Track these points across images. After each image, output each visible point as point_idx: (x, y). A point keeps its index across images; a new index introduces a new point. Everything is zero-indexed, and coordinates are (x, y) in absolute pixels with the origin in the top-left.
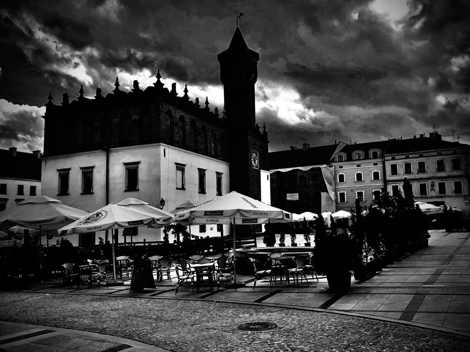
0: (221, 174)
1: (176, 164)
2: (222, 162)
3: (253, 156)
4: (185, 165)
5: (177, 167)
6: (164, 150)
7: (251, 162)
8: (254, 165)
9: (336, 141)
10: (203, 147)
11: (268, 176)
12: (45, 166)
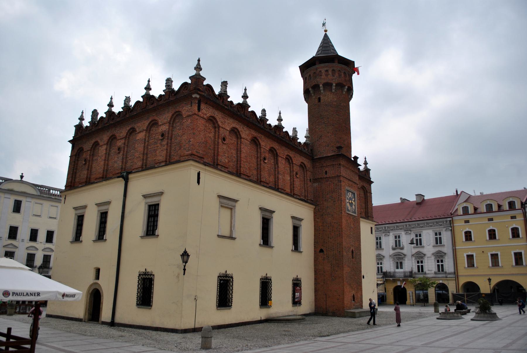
0: (301, 220)
3: (348, 196)
4: (236, 201)
5: (220, 202)
6: (199, 174)
7: (345, 205)
8: (349, 208)
9: (457, 191)
10: (272, 179)
11: (371, 228)
12: (64, 203)
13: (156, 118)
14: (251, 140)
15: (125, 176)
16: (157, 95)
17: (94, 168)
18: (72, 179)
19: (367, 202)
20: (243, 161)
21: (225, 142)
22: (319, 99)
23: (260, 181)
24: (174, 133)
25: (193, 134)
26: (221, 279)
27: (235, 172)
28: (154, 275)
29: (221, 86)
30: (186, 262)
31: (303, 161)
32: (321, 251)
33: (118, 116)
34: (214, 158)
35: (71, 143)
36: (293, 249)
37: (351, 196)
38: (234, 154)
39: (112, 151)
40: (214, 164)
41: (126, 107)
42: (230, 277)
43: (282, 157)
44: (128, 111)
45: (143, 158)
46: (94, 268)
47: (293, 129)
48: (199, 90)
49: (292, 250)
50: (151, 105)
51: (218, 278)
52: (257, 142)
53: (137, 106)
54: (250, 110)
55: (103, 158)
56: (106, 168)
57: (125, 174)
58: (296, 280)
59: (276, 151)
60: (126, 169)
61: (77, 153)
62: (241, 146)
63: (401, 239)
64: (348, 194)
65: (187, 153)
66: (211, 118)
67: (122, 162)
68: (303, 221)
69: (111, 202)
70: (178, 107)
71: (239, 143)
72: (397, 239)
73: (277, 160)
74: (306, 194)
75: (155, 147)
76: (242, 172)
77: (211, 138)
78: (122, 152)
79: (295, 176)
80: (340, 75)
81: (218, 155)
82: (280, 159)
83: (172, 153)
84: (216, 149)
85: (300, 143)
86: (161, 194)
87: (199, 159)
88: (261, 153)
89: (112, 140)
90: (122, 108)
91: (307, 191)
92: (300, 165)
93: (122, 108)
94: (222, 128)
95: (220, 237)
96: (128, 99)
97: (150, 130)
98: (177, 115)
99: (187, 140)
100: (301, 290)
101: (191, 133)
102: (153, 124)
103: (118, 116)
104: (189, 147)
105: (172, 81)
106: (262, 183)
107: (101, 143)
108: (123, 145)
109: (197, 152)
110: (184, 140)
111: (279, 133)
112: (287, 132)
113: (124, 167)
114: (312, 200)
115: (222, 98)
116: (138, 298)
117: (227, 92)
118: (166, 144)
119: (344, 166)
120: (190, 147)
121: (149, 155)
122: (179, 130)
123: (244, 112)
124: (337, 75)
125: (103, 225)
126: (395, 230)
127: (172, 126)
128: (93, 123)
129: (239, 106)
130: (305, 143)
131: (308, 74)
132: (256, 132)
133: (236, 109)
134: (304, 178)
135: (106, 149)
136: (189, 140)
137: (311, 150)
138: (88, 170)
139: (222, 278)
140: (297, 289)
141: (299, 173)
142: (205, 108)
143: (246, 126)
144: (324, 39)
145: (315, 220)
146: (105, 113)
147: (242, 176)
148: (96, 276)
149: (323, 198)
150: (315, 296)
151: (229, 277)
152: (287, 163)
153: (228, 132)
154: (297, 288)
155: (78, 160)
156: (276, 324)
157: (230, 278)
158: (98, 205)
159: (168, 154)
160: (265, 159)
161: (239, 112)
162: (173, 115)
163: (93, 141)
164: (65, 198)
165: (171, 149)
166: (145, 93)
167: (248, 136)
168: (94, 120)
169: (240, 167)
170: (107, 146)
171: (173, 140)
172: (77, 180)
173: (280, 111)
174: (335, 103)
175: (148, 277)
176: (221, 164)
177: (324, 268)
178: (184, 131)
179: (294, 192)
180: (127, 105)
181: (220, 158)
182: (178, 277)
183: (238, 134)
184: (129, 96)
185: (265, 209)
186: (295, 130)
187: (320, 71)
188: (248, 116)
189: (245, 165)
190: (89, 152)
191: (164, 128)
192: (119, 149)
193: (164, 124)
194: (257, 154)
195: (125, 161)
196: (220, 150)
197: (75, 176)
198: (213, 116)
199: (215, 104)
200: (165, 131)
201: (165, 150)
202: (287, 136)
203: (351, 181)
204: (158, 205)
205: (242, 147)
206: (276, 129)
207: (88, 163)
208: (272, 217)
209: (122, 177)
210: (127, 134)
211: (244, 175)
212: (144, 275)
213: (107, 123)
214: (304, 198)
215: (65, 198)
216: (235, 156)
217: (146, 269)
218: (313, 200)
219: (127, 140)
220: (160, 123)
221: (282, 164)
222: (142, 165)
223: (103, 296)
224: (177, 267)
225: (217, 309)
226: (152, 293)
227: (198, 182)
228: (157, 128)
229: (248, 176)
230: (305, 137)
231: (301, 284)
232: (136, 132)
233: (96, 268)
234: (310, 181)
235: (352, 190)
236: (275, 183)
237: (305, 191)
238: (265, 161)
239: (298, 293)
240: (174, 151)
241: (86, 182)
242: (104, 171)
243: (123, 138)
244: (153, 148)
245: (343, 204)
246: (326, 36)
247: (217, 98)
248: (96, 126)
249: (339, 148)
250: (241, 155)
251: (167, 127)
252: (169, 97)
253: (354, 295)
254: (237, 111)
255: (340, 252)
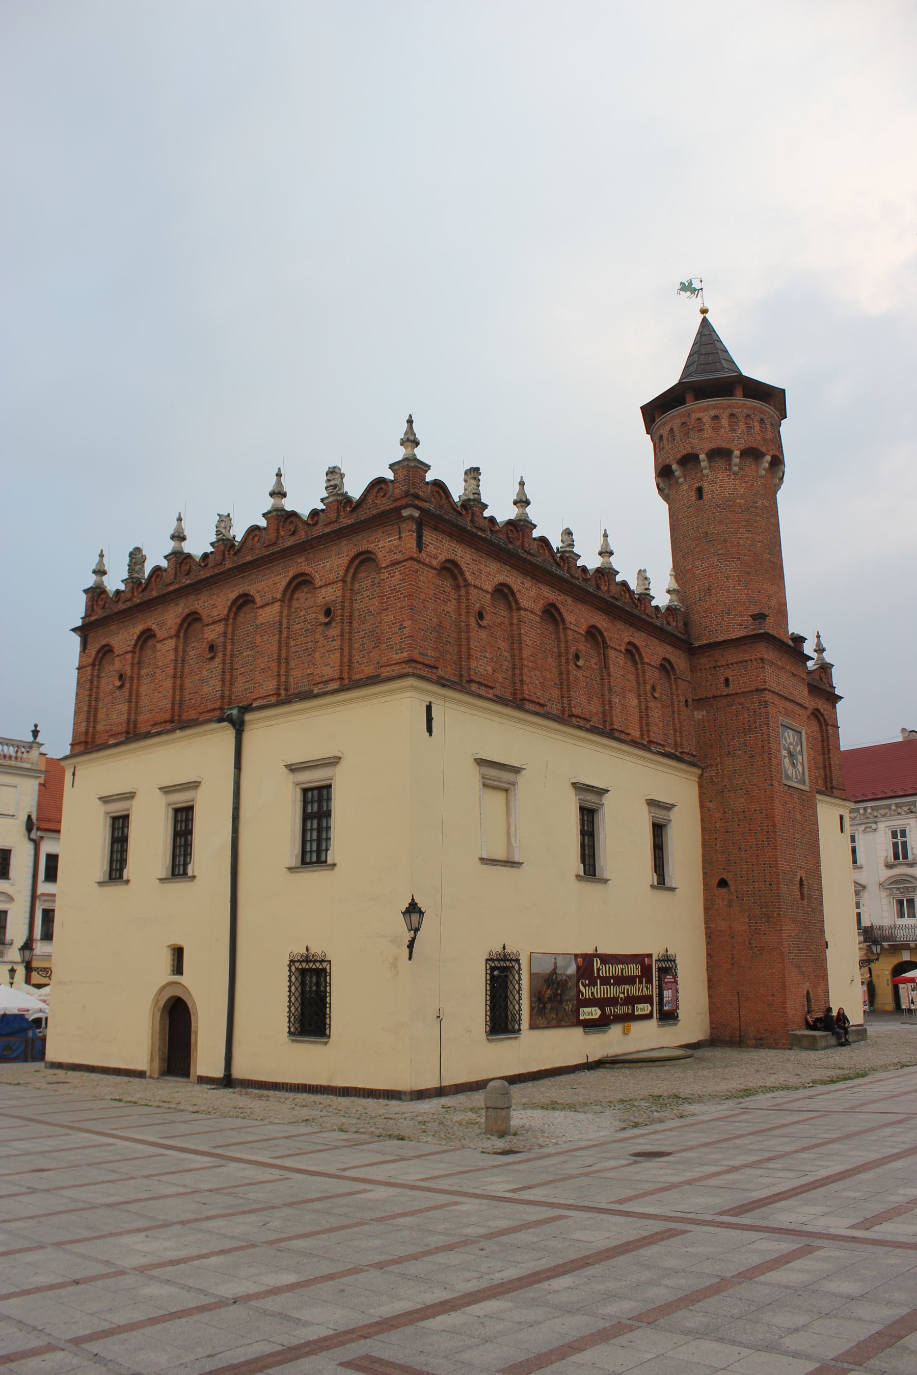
0: (669, 807)
1: (481, 762)
2: (671, 766)
3: (786, 741)
4: (516, 770)
6: (429, 708)
7: (779, 764)
8: (790, 772)
10: (595, 707)
11: (841, 817)
12: (73, 786)
13: (307, 569)
14: (543, 613)
15: (235, 718)
16: (304, 512)
17: (146, 695)
18: (88, 726)
19: (829, 750)
20: (527, 666)
21: (484, 623)
22: (700, 491)
23: (569, 716)
24: (356, 606)
25: (410, 609)
26: (493, 965)
27: (509, 696)
28: (330, 961)
29: (466, 481)
30: (416, 930)
31: (667, 656)
32: (723, 883)
33: (202, 564)
34: (461, 665)
35: (80, 633)
36: (653, 883)
37: (791, 740)
38: (505, 651)
39: (191, 654)
40: (461, 681)
41: (224, 544)
42: (514, 960)
43: (618, 648)
44: (229, 551)
45: (279, 672)
46: (169, 946)
47: (638, 574)
48: (417, 497)
49: (652, 886)
50: (291, 535)
51: (486, 963)
52: (556, 614)
53: (253, 540)
54: (536, 534)
55: (170, 671)
56: (178, 698)
57: (235, 712)
58: (664, 961)
59: (601, 634)
60: (233, 697)
61: (95, 659)
62: (519, 629)
63: (908, 839)
64: (786, 734)
65: (398, 656)
66: (448, 565)
67: (223, 681)
68: (675, 809)
69: (200, 782)
70: (365, 542)
71: (515, 621)
72: (899, 840)
73: (606, 658)
74: (678, 739)
75: (308, 642)
76: (528, 694)
77: (449, 616)
78: (220, 655)
79: (649, 694)
80: (751, 428)
81: (469, 656)
82: (612, 654)
83: (354, 656)
84: (464, 642)
85: (657, 607)
86: (334, 761)
87: (428, 671)
88: (566, 641)
89: (190, 624)
90: (212, 544)
91: (681, 733)
92: (662, 665)
93: (212, 544)
94: (476, 587)
95: (486, 864)
96: (225, 521)
97: (291, 599)
98: (362, 562)
99: (396, 623)
100: (676, 982)
101: (405, 607)
102: (299, 585)
103: (202, 564)
104: (402, 642)
105: (342, 476)
106: (574, 720)
107: (160, 634)
108: (222, 639)
109: (420, 654)
110: (387, 625)
111: (606, 588)
112: (624, 584)
113: (227, 693)
114: (693, 755)
115: (470, 511)
116: (292, 1019)
117: (479, 494)
118: (337, 636)
119: (772, 664)
120: (405, 641)
121: (292, 664)
122: (369, 599)
123: (523, 541)
124: (742, 426)
125: (183, 840)
126: (891, 815)
127: (351, 590)
128: (133, 581)
129: (511, 528)
130: (669, 608)
131: (668, 428)
132: (554, 590)
133: (503, 536)
134: (672, 699)
135: (176, 649)
136: (401, 625)
137: (685, 624)
138: (130, 701)
139: (496, 963)
140: (666, 980)
141: (658, 688)
142: (432, 540)
143: (529, 578)
144: (700, 333)
145: (702, 806)
146: (165, 557)
147: (529, 706)
148: (173, 966)
149: (720, 747)
150: (710, 997)
151: (511, 960)
152: (629, 664)
153: (489, 596)
154: (668, 977)
155: (98, 677)
156: (628, 1072)
157: (514, 963)
158: (167, 790)
159: (346, 660)
160: (577, 657)
161: (511, 542)
162: (352, 561)
163: (138, 629)
164: (74, 774)
165: (350, 646)
166: (271, 506)
167: (534, 602)
168: (136, 575)
169: (521, 681)
170: (177, 641)
171: (355, 625)
172: (100, 727)
173: (605, 530)
174: (742, 501)
175: (314, 967)
176: (478, 680)
177: (731, 928)
178: (384, 603)
179: (649, 737)
180: (224, 535)
181: (474, 664)
182: (394, 965)
183: (511, 598)
184: (229, 515)
185: (584, 785)
186: (642, 575)
187: (699, 419)
188: (531, 551)
189: (531, 677)
190: (129, 656)
191: (330, 594)
192: (212, 648)
193: (330, 584)
194: (559, 646)
195: (228, 678)
196: (472, 646)
197: (95, 716)
198: (453, 558)
199: (455, 529)
200: (333, 601)
201: (335, 650)
202: (625, 593)
203: (791, 701)
204: (329, 787)
205: (523, 631)
206: (600, 577)
207: (128, 685)
208: (602, 805)
209: (230, 719)
210: (230, 611)
211: (532, 702)
212: (303, 961)
213: (171, 584)
214: (673, 751)
215: (74, 774)
216: (507, 654)
217: (307, 947)
218: (694, 753)
219: (230, 626)
220: (318, 583)
221: (618, 662)
222: (278, 689)
223: (196, 1014)
224: (391, 941)
225: (488, 1040)
226: (328, 1005)
227: (430, 730)
228: (309, 595)
229: (542, 705)
230: (668, 592)
231: (675, 970)
232: (256, 606)
233: (173, 947)
234: (687, 706)
235: (794, 724)
236: (604, 716)
237: (675, 731)
238: (578, 663)
239: (670, 991)
240: (361, 651)
241: (128, 732)
242: (173, 704)
243: (220, 621)
244: (301, 644)
245: (774, 762)
246: (705, 323)
247: (455, 510)
248: (144, 590)
249: (760, 617)
250: (521, 653)
251: (339, 593)
252: (338, 516)
253: (808, 992)
254: (507, 540)
255: (771, 884)
